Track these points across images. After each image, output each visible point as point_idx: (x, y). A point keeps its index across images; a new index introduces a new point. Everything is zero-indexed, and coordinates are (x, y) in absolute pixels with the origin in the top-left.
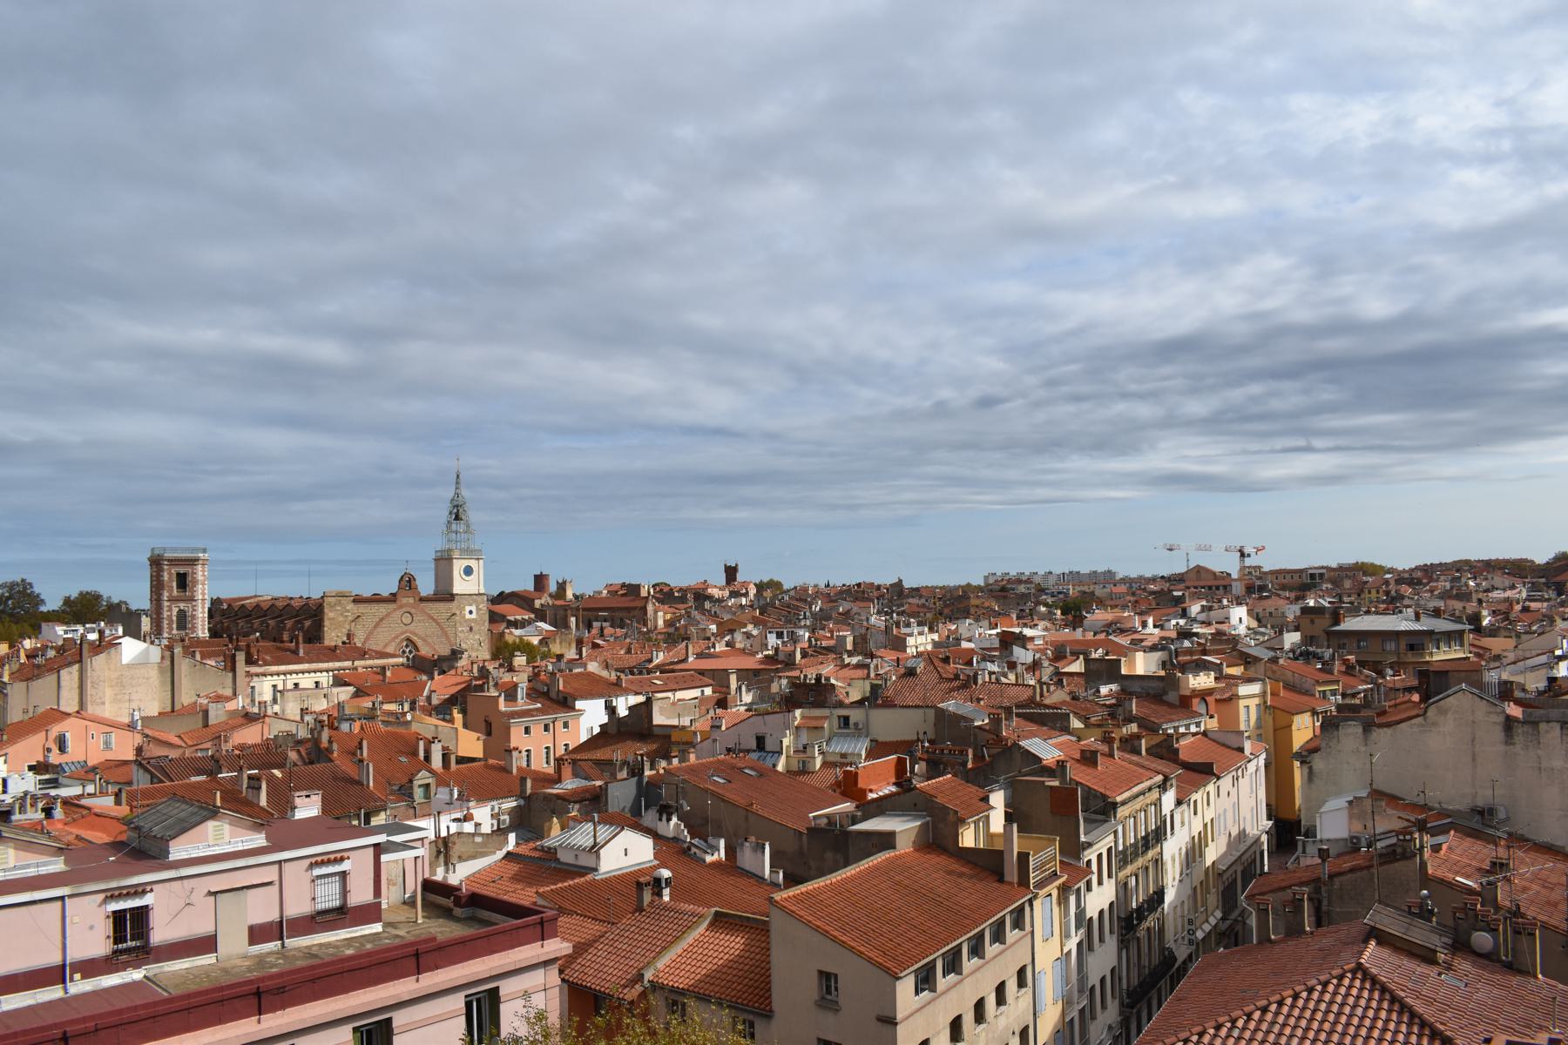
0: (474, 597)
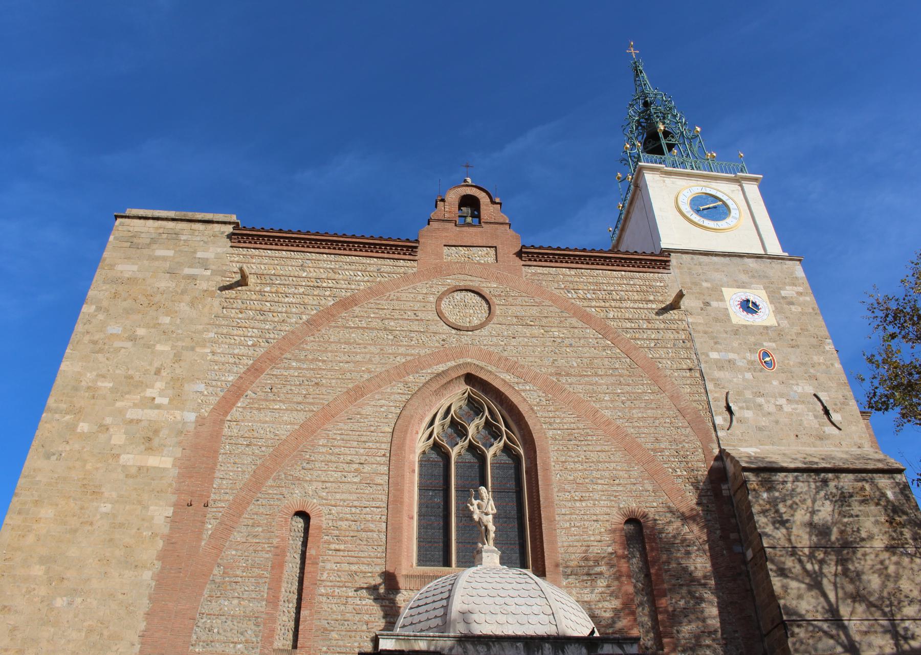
0: (751, 262)
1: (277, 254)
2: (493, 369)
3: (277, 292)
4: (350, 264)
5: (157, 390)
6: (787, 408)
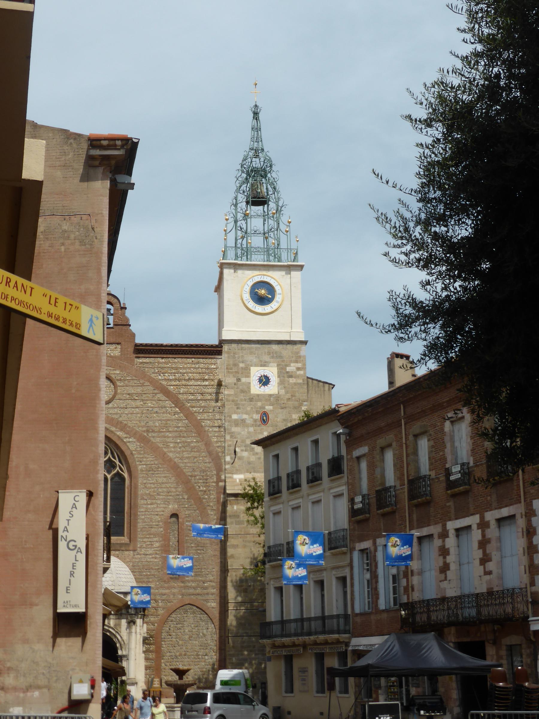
0: (275, 347)
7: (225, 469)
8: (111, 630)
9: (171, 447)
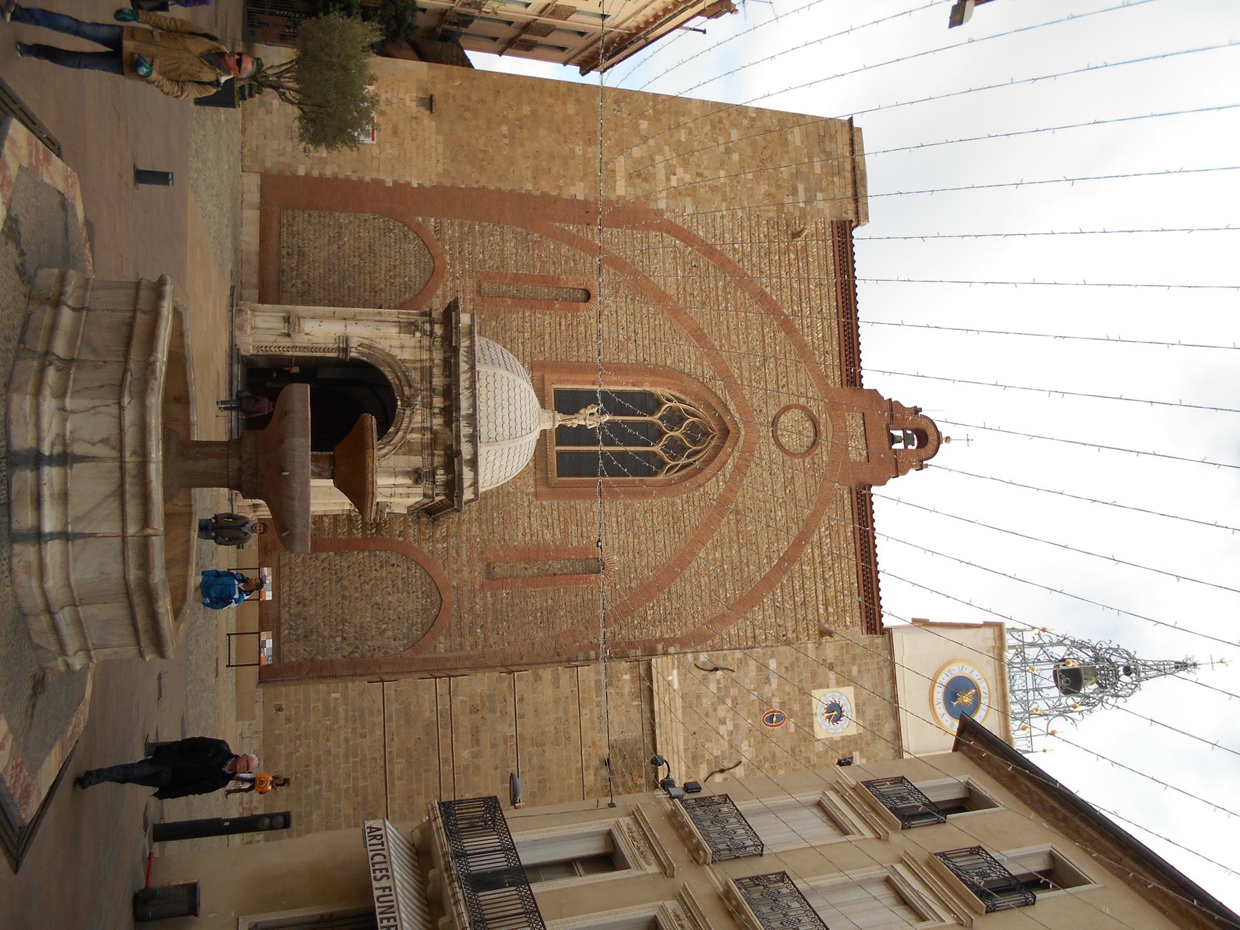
1: (830, 261)
2: (736, 454)
3: (790, 265)
4: (830, 326)
5: (682, 176)
6: (723, 730)
7: (685, 653)
8: (400, 433)
9: (715, 554)
